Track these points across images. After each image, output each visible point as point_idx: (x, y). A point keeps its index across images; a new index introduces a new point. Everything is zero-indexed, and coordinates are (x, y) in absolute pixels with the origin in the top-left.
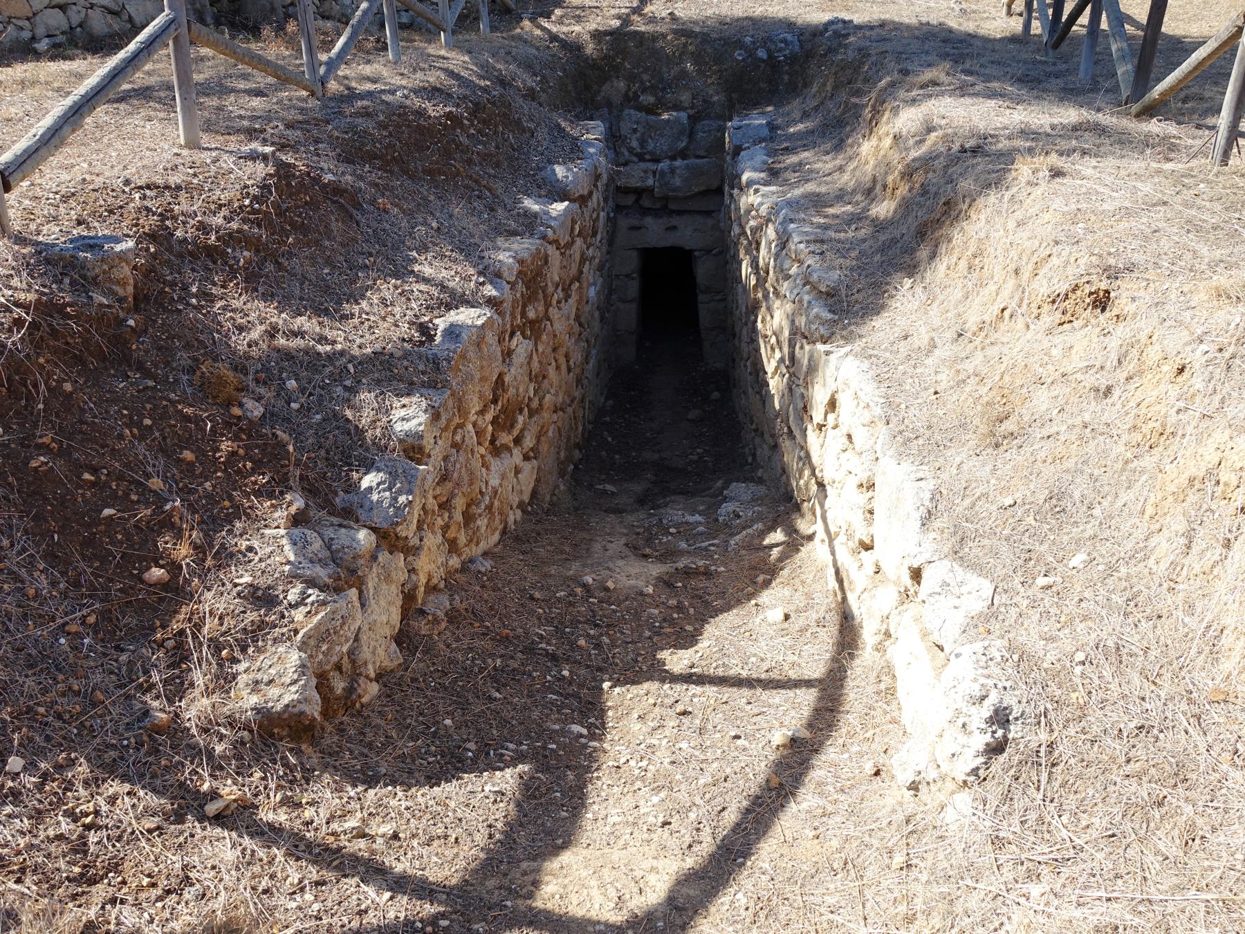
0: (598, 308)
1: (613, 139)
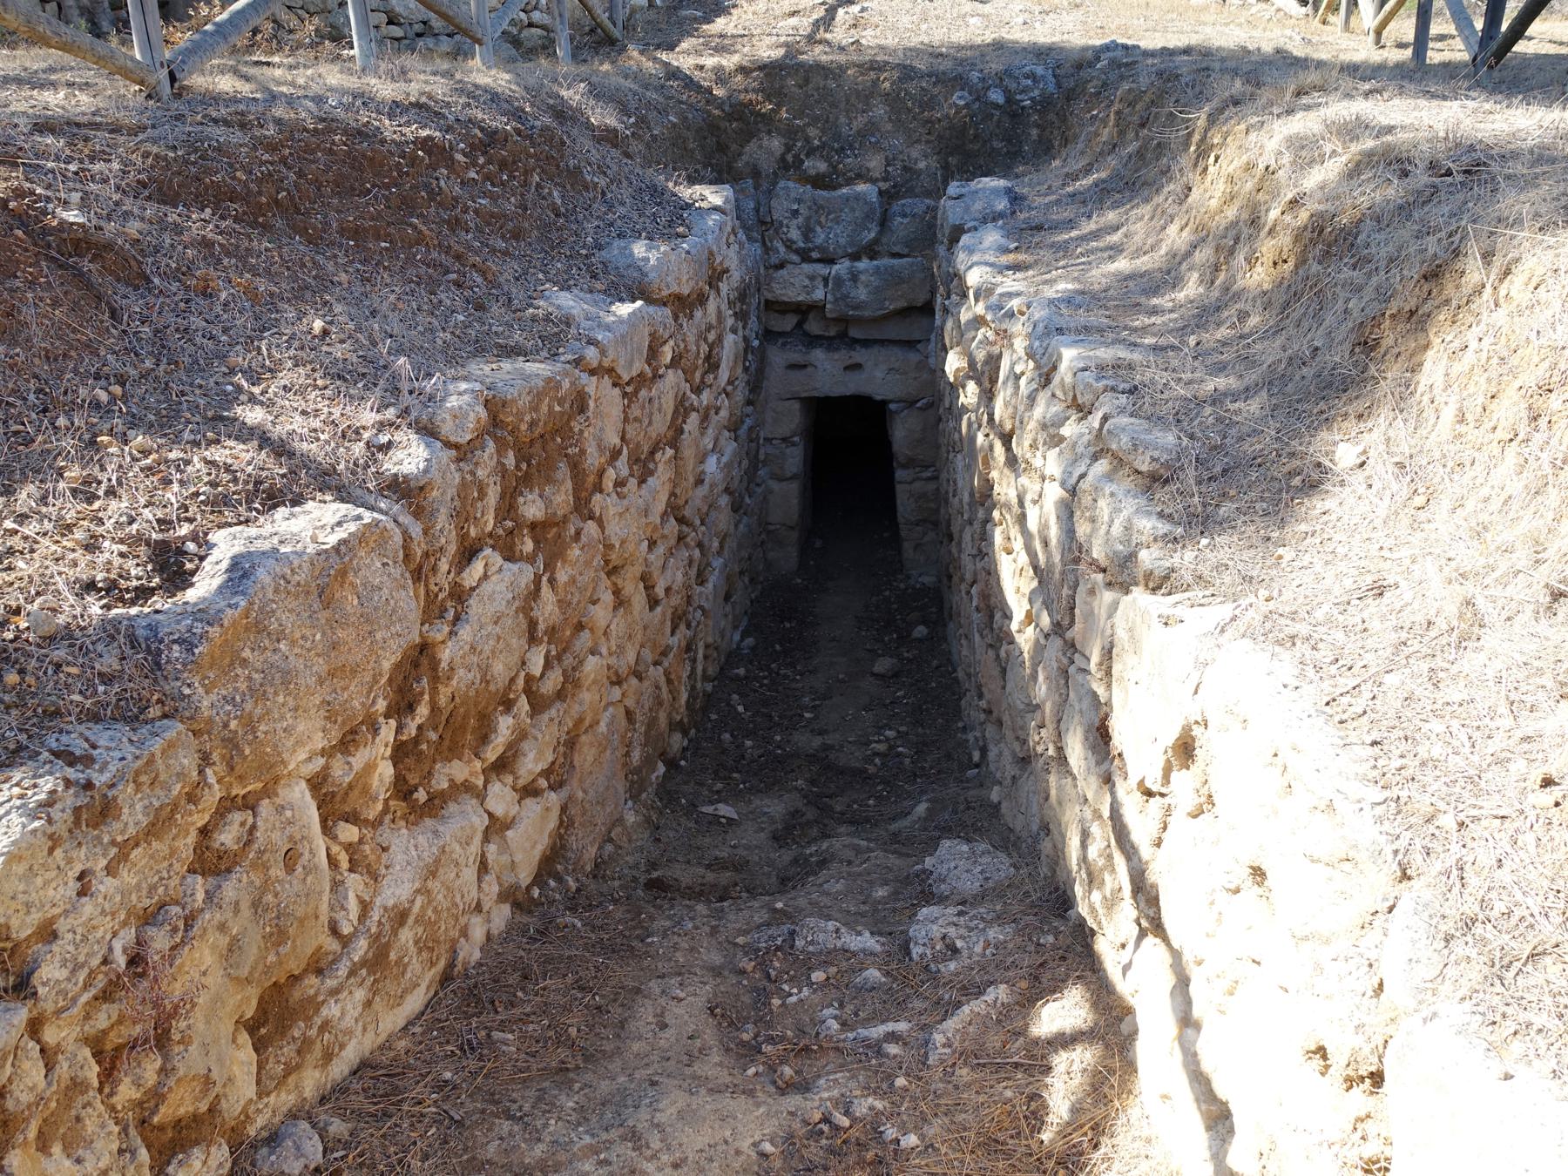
0: (727, 490)
1: (756, 223)
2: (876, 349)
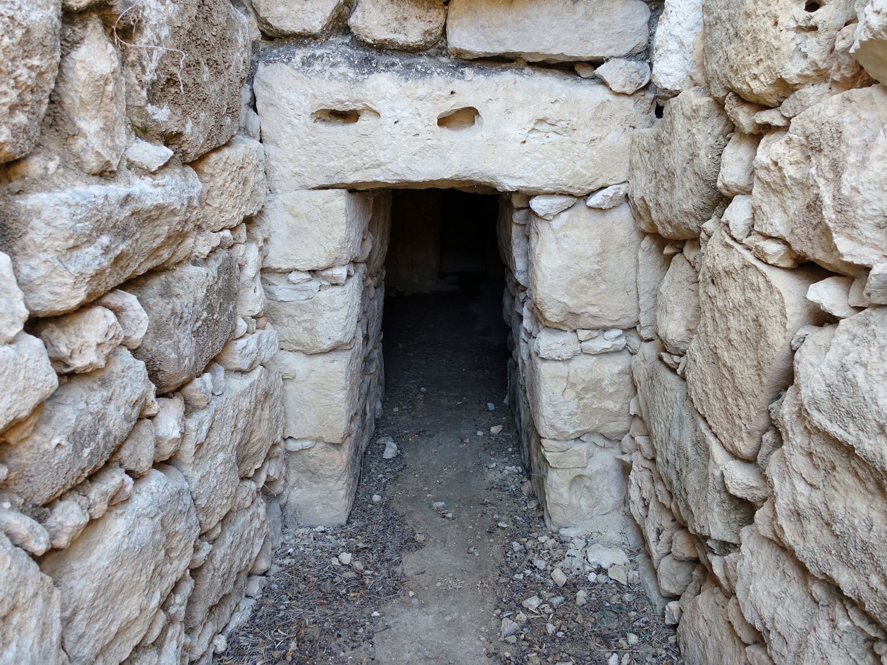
2: (507, 77)
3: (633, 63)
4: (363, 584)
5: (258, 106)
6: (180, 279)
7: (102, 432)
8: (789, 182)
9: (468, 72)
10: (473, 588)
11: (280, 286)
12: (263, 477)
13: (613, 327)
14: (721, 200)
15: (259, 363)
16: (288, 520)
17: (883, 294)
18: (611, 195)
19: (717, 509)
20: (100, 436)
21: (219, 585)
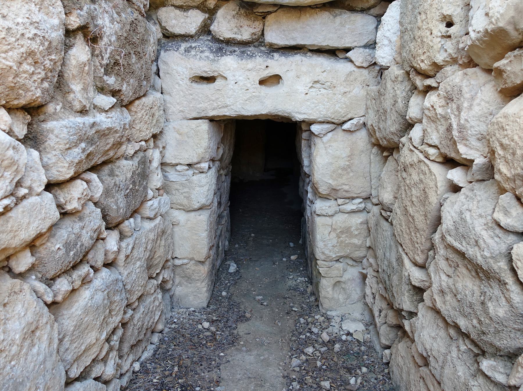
2: (298, 58)
3: (367, 50)
4: (215, 339)
5: (161, 74)
6: (119, 167)
7: (79, 244)
8: (439, 117)
9: (276, 55)
10: (277, 342)
11: (171, 173)
12: (161, 278)
13: (357, 197)
14: (409, 126)
15: (159, 214)
16: (174, 304)
17: (480, 174)
18: (355, 123)
19: (407, 294)
20: (78, 246)
21: (137, 334)
